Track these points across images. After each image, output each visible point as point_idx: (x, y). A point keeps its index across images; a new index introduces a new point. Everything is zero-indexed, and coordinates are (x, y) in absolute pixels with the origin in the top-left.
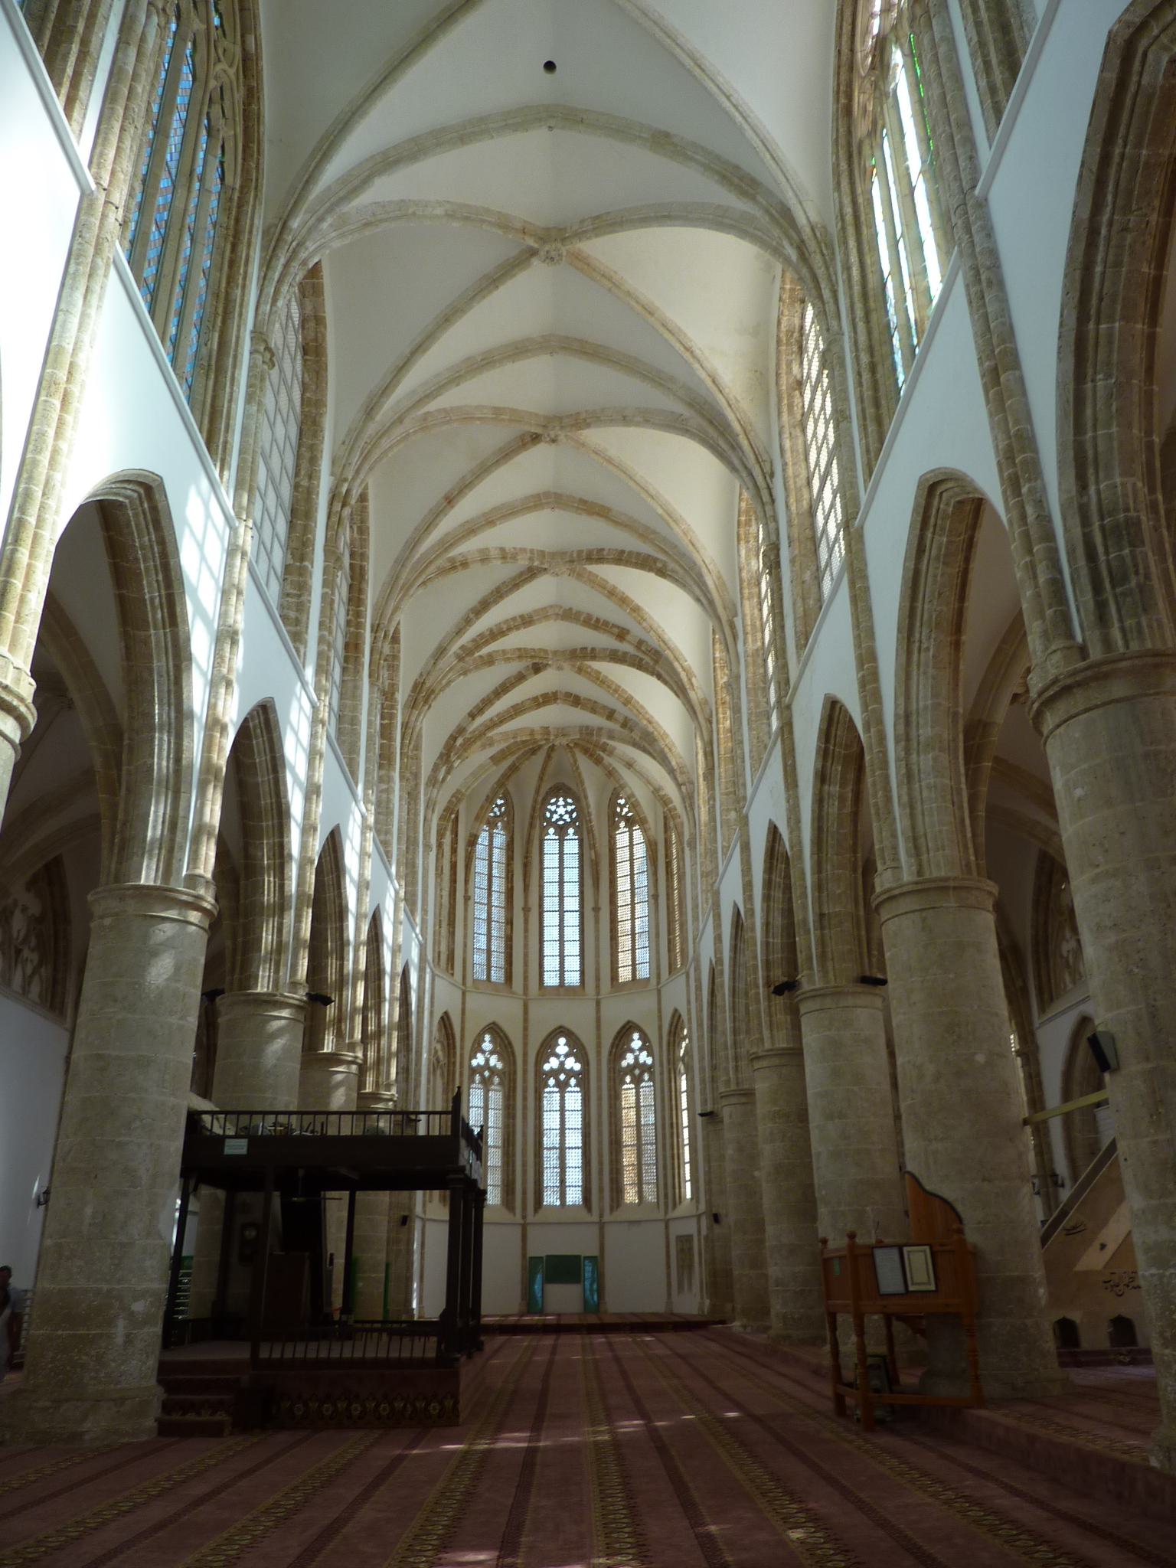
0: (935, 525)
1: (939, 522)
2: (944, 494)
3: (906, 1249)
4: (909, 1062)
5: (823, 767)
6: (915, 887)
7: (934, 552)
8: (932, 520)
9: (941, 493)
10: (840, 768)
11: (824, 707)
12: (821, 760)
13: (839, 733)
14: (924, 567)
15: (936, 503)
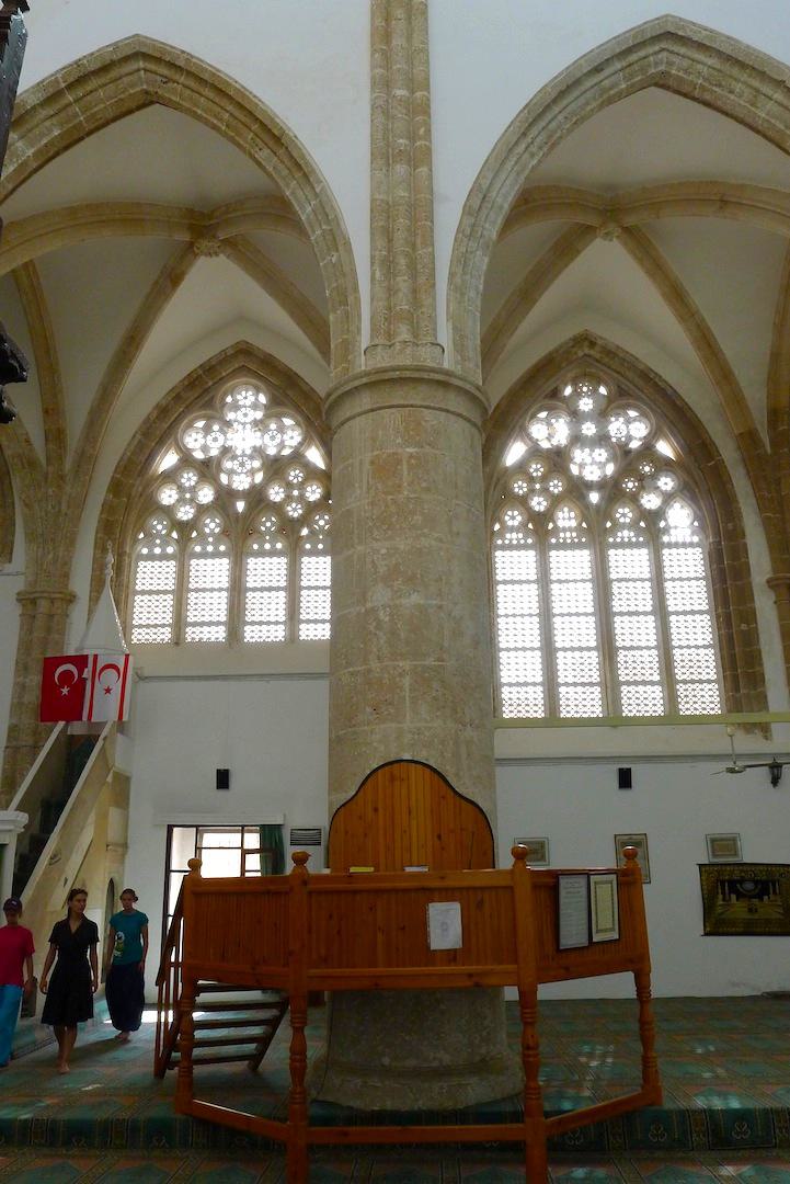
0: (630, 65)
1: (636, 67)
2: (665, 54)
3: (593, 879)
4: (440, 607)
5: (34, 108)
6: (473, 391)
7: (606, 83)
8: (633, 57)
9: (663, 50)
10: (56, 132)
11: (116, 46)
12: (41, 96)
13: (101, 92)
14: (588, 84)
15: (650, 50)
